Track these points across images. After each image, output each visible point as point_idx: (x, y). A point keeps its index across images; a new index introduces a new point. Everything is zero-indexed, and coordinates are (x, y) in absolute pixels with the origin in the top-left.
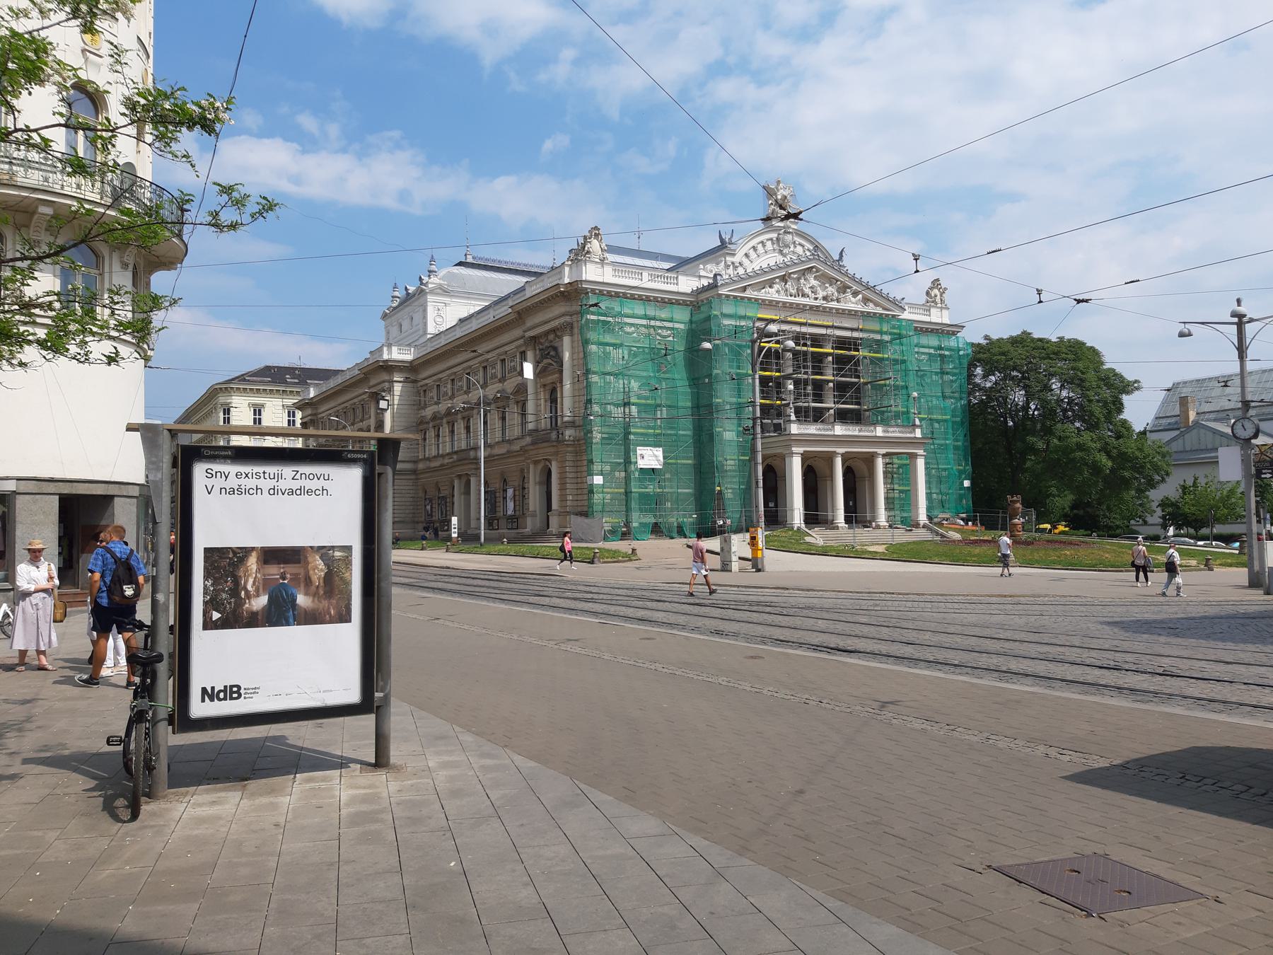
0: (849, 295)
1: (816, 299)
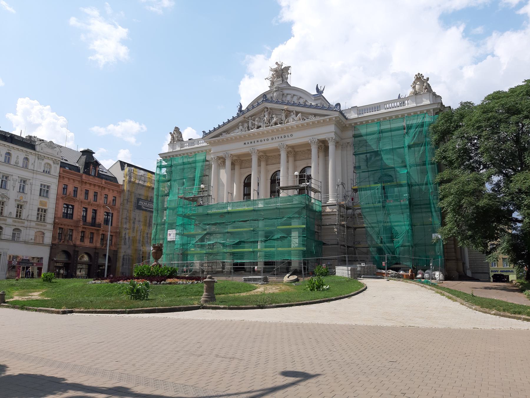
1: (269, 126)
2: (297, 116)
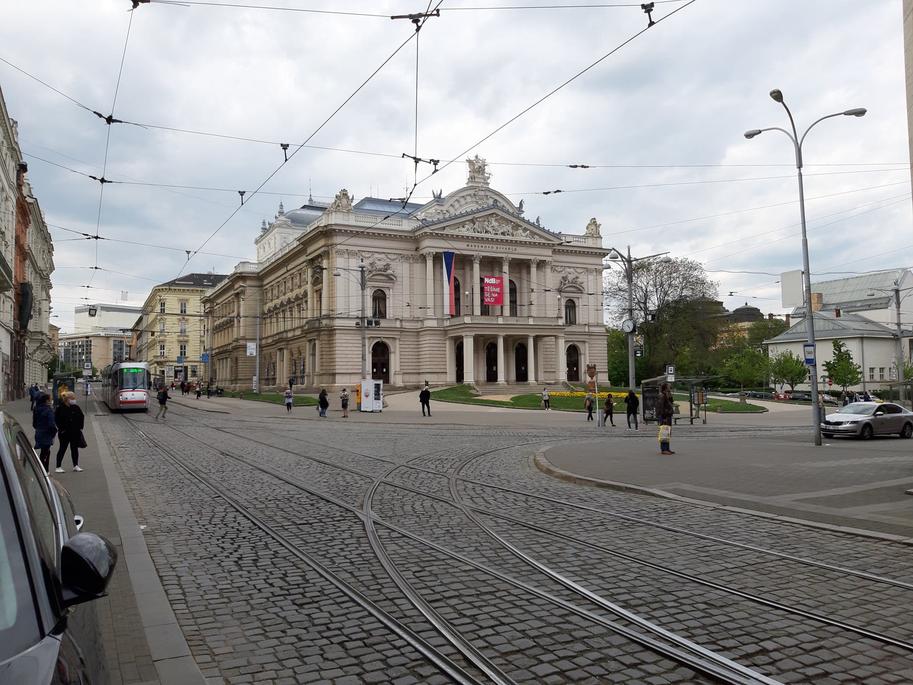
1: (497, 234)
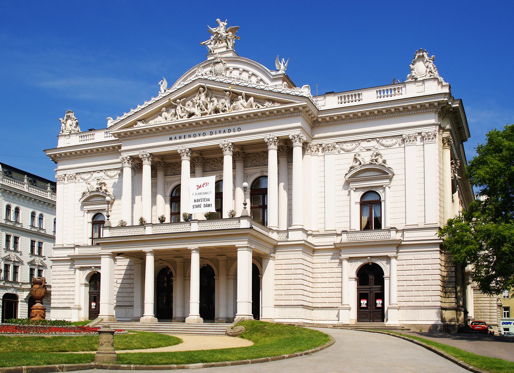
0: (242, 101)
1: (206, 114)
2: (247, 100)
